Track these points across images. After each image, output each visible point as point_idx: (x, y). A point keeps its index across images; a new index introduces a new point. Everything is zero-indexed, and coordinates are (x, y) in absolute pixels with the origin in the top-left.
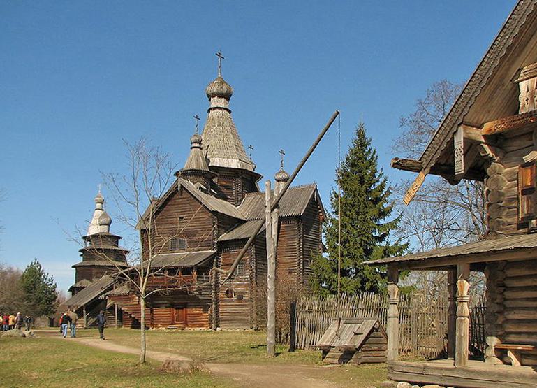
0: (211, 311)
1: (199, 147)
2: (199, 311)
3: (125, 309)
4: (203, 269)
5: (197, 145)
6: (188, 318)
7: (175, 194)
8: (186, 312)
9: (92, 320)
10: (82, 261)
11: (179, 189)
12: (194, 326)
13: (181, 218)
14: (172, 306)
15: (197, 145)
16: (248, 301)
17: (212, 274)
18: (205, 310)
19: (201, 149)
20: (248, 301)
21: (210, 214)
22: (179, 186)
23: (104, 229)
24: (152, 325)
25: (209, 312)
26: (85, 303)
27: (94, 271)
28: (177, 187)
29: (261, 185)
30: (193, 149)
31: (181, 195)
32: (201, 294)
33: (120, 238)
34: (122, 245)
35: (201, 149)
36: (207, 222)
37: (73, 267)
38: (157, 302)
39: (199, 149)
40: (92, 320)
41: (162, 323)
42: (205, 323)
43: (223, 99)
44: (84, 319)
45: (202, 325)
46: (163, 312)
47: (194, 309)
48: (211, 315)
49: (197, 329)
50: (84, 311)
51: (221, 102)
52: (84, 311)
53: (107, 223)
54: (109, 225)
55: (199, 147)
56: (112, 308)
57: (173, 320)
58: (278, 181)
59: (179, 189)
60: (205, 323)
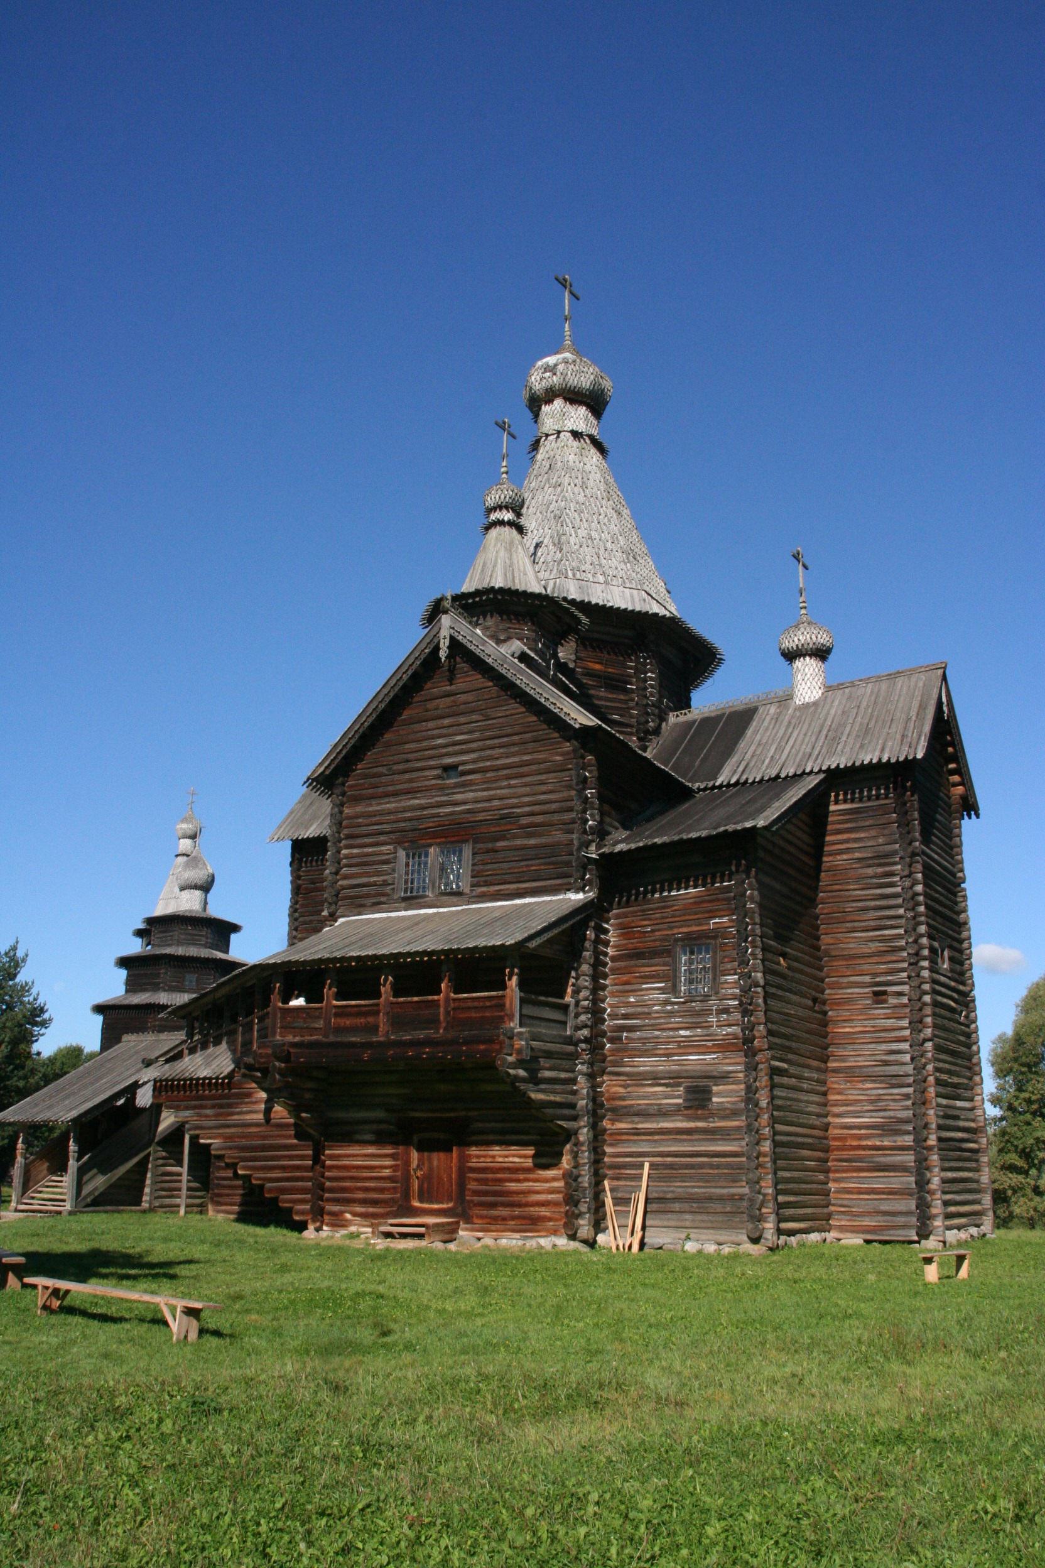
0: (575, 1156)
1: (510, 524)
2: (519, 1156)
4: (546, 965)
5: (508, 516)
6: (472, 1186)
7: (423, 674)
8: (464, 1159)
9: (98, 1182)
10: (123, 992)
11: (443, 654)
12: (494, 1224)
13: (448, 769)
14: (399, 1133)
15: (508, 516)
16: (734, 1114)
17: (576, 990)
18: (547, 1157)
19: (520, 530)
20: (734, 1114)
21: (568, 747)
22: (444, 644)
23: (189, 903)
24: (319, 1214)
25: (566, 1162)
28: (437, 648)
31: (451, 681)
32: (535, 1080)
33: (235, 928)
35: (520, 530)
36: (551, 778)
37: (99, 1009)
38: (341, 1115)
39: (514, 532)
40: (98, 1182)
41: (359, 1209)
42: (544, 1212)
43: (582, 410)
44: (68, 1180)
45: (531, 1224)
46: (366, 1159)
47: (496, 1151)
48: (571, 1177)
49: (510, 1241)
50: (72, 1147)
51: (579, 418)
52: (72, 1147)
53: (199, 883)
54: (206, 887)
55: (510, 524)
56: (174, 1137)
57: (407, 1196)
58: (791, 656)
59: (443, 654)
60: (544, 1212)
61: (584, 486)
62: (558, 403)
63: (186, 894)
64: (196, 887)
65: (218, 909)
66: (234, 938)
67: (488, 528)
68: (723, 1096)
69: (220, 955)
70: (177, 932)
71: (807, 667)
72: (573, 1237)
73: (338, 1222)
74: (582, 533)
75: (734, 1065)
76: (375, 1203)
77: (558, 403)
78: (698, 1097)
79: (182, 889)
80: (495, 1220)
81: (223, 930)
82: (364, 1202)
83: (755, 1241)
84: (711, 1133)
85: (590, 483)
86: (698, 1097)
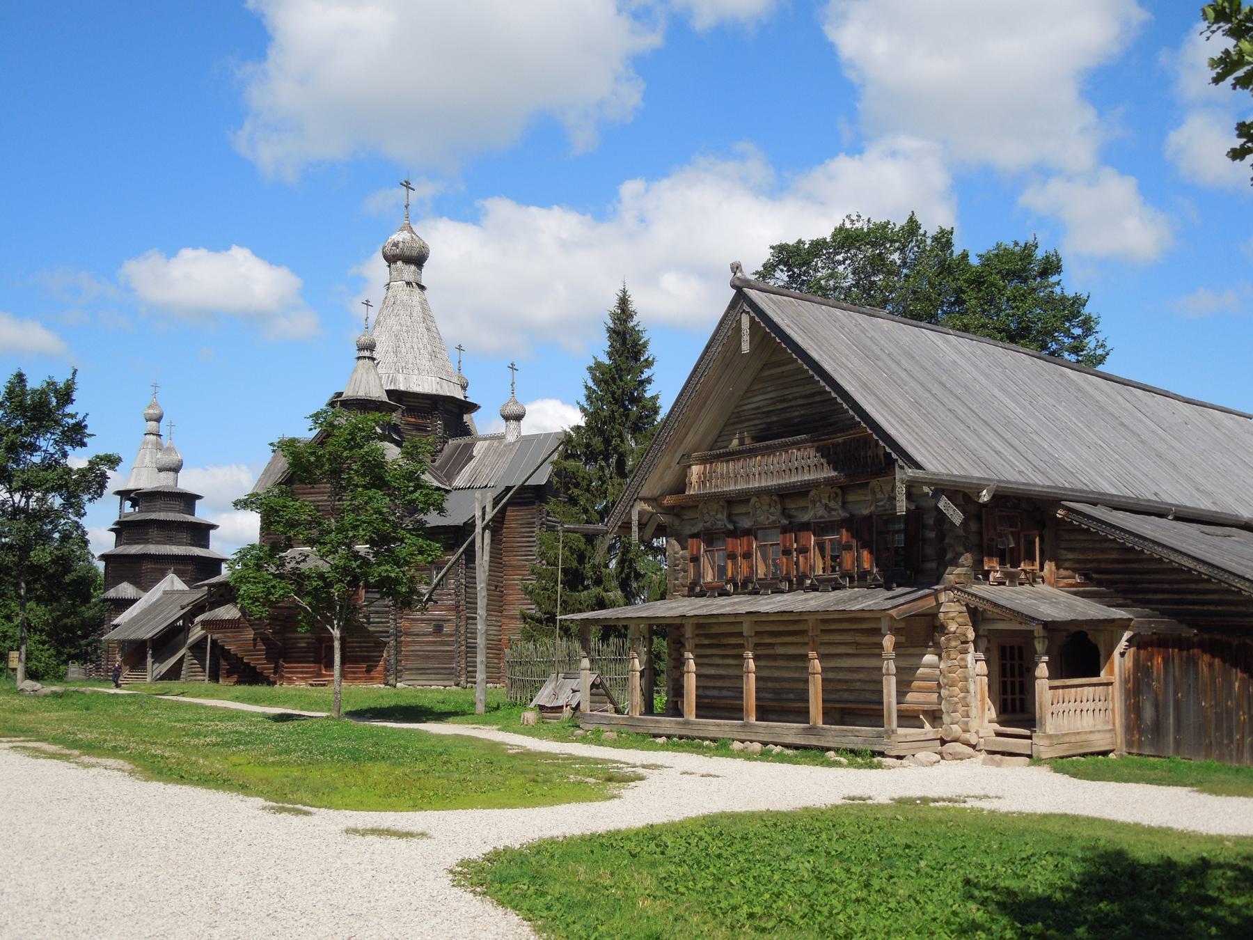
3: (232, 648)
5: (367, 354)
15: (367, 354)
16: (452, 635)
26: (150, 635)
27: (147, 566)
29: (475, 421)
30: (361, 362)
32: (369, 623)
34: (202, 514)
43: (413, 267)
54: (176, 469)
61: (411, 316)
62: (399, 263)
63: (163, 474)
64: (170, 470)
65: (186, 482)
66: (197, 502)
67: (359, 358)
68: (447, 629)
69: (190, 518)
70: (159, 503)
71: (513, 424)
72: (386, 684)
73: (290, 681)
74: (408, 345)
75: (451, 616)
76: (307, 673)
77: (399, 263)
78: (438, 629)
79: (160, 470)
80: (356, 679)
81: (189, 500)
82: (302, 673)
83: (457, 685)
84: (443, 643)
85: (415, 314)
86: (438, 629)
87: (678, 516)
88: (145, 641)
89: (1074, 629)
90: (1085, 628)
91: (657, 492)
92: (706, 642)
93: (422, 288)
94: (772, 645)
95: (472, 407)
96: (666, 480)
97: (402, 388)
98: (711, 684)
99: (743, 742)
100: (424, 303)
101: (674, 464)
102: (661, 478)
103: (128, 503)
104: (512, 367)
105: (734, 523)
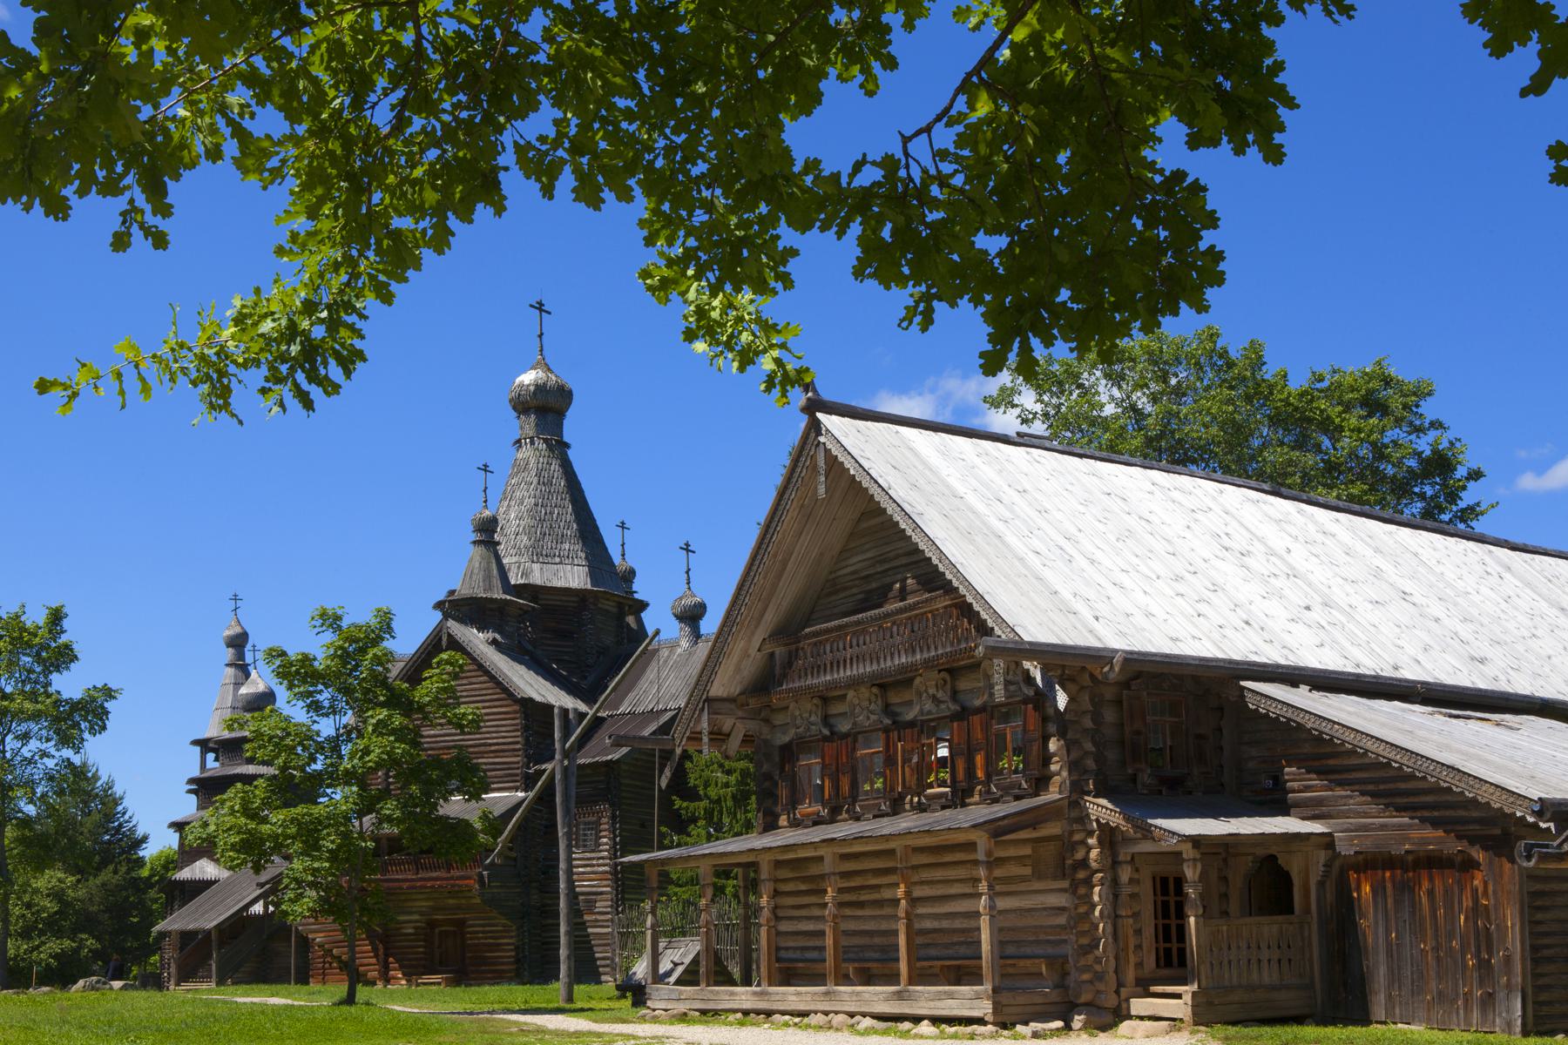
22: (445, 639)
26: (215, 923)
87: (767, 721)
88: (208, 933)
89: (1261, 852)
90: (1273, 850)
91: (735, 690)
92: (803, 887)
93: (567, 446)
94: (877, 887)
95: (643, 605)
96: (746, 673)
97: (539, 582)
98: (811, 944)
99: (826, 1013)
100: (567, 467)
101: (753, 651)
102: (738, 669)
103: (211, 756)
104: (687, 548)
105: (830, 727)
